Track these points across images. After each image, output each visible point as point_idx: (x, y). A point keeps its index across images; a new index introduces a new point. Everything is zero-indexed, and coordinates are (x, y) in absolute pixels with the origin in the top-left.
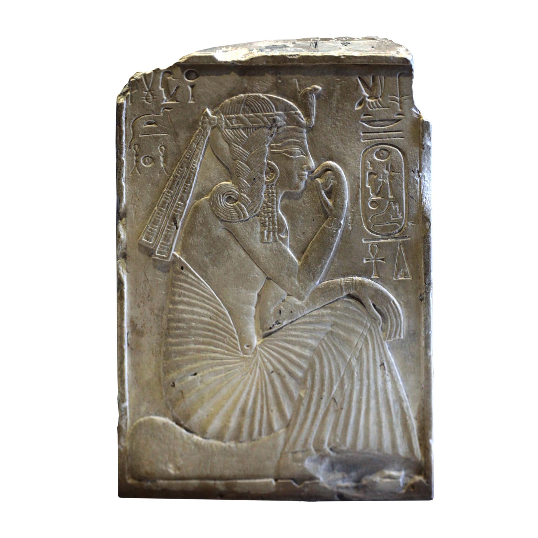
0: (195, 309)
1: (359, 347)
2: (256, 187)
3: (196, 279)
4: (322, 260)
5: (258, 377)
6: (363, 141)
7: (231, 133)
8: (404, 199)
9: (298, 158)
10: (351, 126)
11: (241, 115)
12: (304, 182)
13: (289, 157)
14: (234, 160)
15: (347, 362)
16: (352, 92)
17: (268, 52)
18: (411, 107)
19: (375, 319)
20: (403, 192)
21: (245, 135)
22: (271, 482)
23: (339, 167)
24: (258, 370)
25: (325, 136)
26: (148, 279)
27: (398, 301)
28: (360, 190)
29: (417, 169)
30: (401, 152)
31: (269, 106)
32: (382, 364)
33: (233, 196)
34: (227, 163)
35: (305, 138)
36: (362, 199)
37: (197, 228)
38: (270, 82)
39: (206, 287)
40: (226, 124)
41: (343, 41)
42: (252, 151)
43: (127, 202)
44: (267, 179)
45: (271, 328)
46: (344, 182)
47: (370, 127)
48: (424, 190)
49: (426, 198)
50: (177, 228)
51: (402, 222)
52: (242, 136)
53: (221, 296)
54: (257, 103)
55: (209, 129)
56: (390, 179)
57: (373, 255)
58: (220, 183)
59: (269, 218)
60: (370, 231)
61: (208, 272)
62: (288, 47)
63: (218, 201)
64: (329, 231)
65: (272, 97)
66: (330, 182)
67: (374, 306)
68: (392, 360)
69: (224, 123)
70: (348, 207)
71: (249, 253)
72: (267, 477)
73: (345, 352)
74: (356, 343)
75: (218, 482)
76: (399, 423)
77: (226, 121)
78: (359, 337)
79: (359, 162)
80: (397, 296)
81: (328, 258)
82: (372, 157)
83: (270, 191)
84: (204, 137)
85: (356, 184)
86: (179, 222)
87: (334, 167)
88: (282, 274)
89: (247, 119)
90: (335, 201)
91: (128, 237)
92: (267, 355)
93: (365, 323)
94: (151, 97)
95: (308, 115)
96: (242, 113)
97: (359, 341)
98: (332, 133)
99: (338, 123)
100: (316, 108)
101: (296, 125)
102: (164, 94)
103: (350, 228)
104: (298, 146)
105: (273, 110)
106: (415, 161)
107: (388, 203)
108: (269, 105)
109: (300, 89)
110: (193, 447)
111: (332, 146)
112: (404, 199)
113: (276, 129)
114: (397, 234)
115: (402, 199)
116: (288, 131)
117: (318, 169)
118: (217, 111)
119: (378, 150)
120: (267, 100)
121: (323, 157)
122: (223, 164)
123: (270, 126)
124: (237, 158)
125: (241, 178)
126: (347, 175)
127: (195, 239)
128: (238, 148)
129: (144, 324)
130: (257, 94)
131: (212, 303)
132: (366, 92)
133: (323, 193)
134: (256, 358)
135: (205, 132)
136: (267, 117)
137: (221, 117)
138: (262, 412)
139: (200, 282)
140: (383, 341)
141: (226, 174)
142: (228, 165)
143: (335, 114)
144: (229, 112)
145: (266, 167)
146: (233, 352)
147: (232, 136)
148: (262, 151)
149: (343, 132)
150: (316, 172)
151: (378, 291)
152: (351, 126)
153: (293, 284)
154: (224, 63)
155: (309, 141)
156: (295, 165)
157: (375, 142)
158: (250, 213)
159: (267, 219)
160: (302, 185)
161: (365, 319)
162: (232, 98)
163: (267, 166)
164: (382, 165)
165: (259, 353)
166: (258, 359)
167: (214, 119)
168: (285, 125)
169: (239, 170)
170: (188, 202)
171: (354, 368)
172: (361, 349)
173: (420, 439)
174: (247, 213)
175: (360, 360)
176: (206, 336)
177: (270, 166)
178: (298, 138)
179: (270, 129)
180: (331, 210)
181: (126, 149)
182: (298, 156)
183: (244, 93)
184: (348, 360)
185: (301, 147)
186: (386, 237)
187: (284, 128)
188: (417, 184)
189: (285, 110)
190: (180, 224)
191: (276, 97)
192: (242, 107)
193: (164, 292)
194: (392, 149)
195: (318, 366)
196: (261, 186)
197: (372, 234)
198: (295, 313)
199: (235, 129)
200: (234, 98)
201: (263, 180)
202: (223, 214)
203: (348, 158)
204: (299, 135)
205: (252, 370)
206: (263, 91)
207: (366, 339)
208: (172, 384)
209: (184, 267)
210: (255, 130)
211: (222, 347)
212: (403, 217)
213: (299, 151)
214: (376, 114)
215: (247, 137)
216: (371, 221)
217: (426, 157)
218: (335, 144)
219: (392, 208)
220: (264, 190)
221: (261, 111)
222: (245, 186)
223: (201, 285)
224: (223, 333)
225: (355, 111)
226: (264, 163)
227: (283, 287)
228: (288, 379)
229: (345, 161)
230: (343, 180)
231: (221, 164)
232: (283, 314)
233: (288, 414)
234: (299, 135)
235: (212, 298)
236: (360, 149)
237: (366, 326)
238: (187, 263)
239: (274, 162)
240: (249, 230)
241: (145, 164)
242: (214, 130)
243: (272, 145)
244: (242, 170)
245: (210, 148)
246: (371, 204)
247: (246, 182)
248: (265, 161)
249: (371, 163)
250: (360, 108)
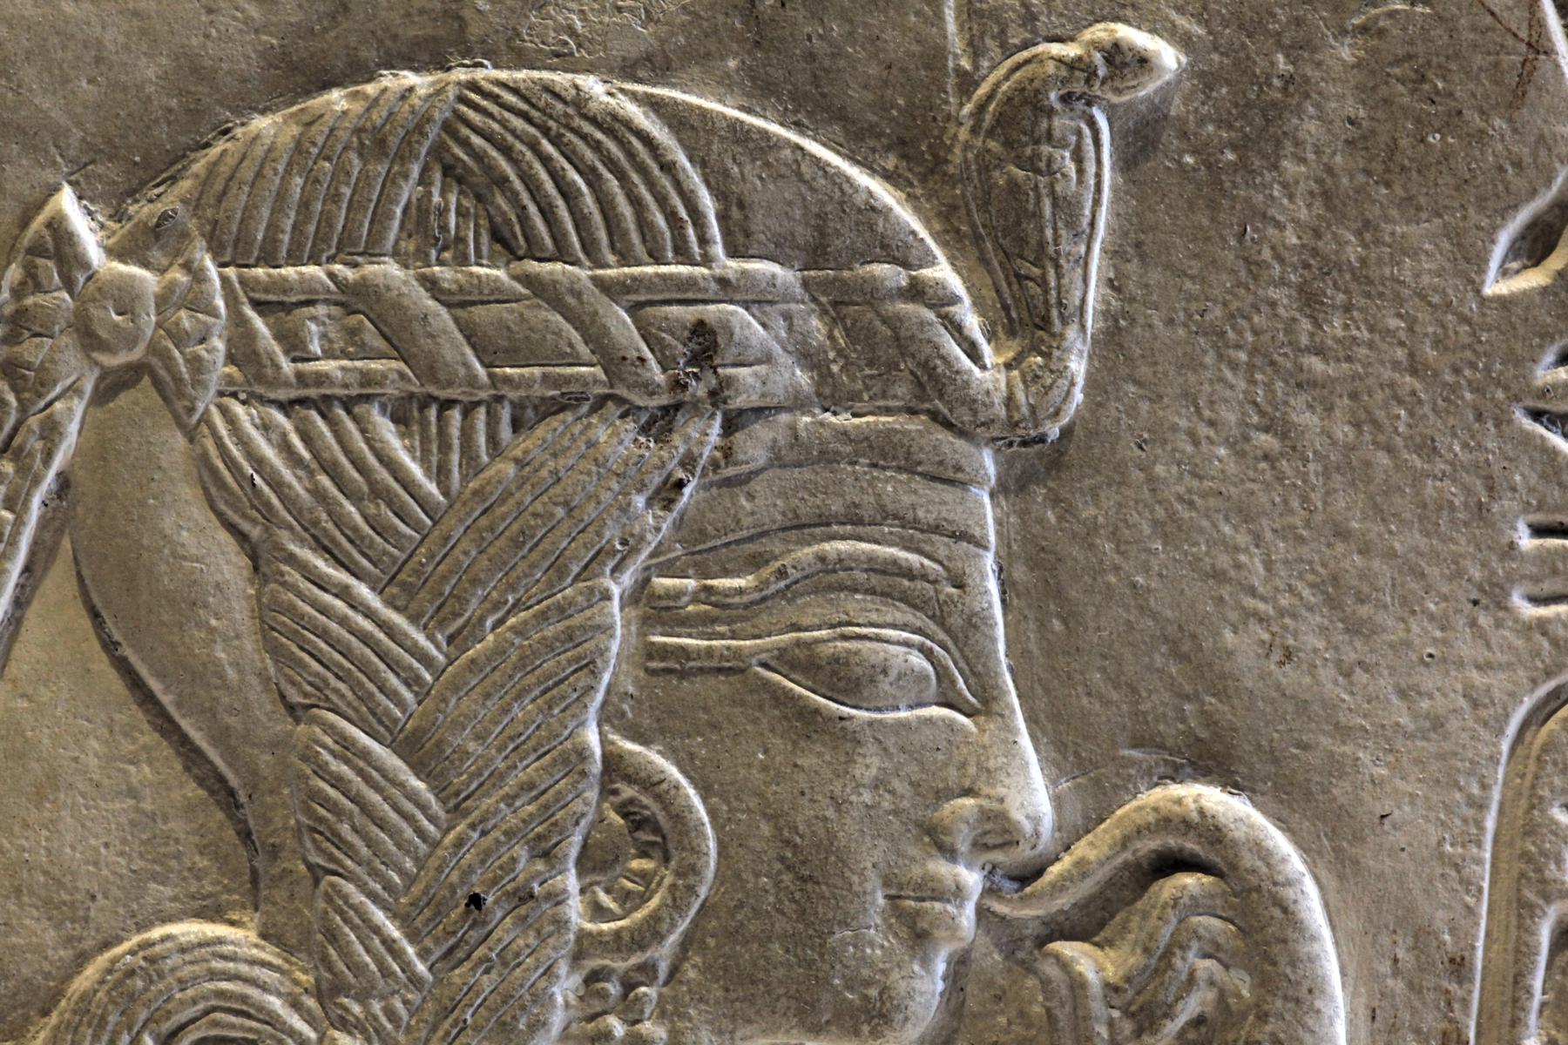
2: (487, 982)
6: (1530, 611)
7: (286, 448)
9: (903, 725)
11: (389, 270)
12: (941, 967)
13: (817, 711)
14: (291, 708)
21: (416, 470)
25: (1171, 529)
31: (662, 201)
34: (221, 736)
35: (986, 548)
40: (243, 352)
42: (473, 630)
44: (598, 912)
46: (1316, 988)
52: (384, 475)
54: (546, 160)
55: (73, 390)
58: (142, 927)
65: (704, 114)
69: (219, 344)
77: (238, 320)
79: (1481, 806)
83: (618, 1028)
84: (22, 470)
87: (1239, 833)
89: (443, 317)
96: (395, 254)
98: (1245, 514)
99: (1306, 419)
100: (1114, 254)
101: (912, 412)
104: (909, 616)
105: (704, 241)
108: (665, 182)
109: (976, 51)
113: (716, 429)
116: (827, 457)
117: (1081, 849)
118: (164, 217)
121: (1137, 744)
122: (183, 743)
123: (664, 400)
124: (320, 686)
125: (350, 888)
126: (1353, 923)
128: (344, 593)
135: (34, 422)
136: (634, 309)
137: (198, 276)
141: (202, 850)
142: (231, 755)
144: (274, 228)
145: (592, 795)
147: (287, 474)
148: (569, 636)
149: (1346, 505)
150: (1059, 887)
152: (1428, 448)
155: (1020, 573)
156: (867, 797)
162: (317, 102)
163: (607, 792)
167: (125, 298)
168: (798, 403)
169: (326, 802)
177: (628, 792)
178: (915, 531)
179: (660, 424)
182: (903, 714)
183: (430, 56)
185: (941, 621)
187: (793, 428)
189: (815, 254)
192: (408, 191)
196: (527, 974)
199: (323, 406)
200: (337, 99)
201: (561, 924)
204: (930, 502)
206: (622, 48)
210: (517, 425)
213: (918, 661)
215: (432, 488)
218: (1262, 619)
220: (557, 1020)
221: (589, 247)
222: (386, 972)
225: (1483, 301)
226: (582, 754)
229: (1341, 791)
230: (1312, 959)
231: (166, 750)
234: (930, 502)
236: (1498, 683)
239: (672, 753)
242: (124, 399)
243: (663, 583)
245: (71, 587)
248: (592, 737)
250: (1533, 279)
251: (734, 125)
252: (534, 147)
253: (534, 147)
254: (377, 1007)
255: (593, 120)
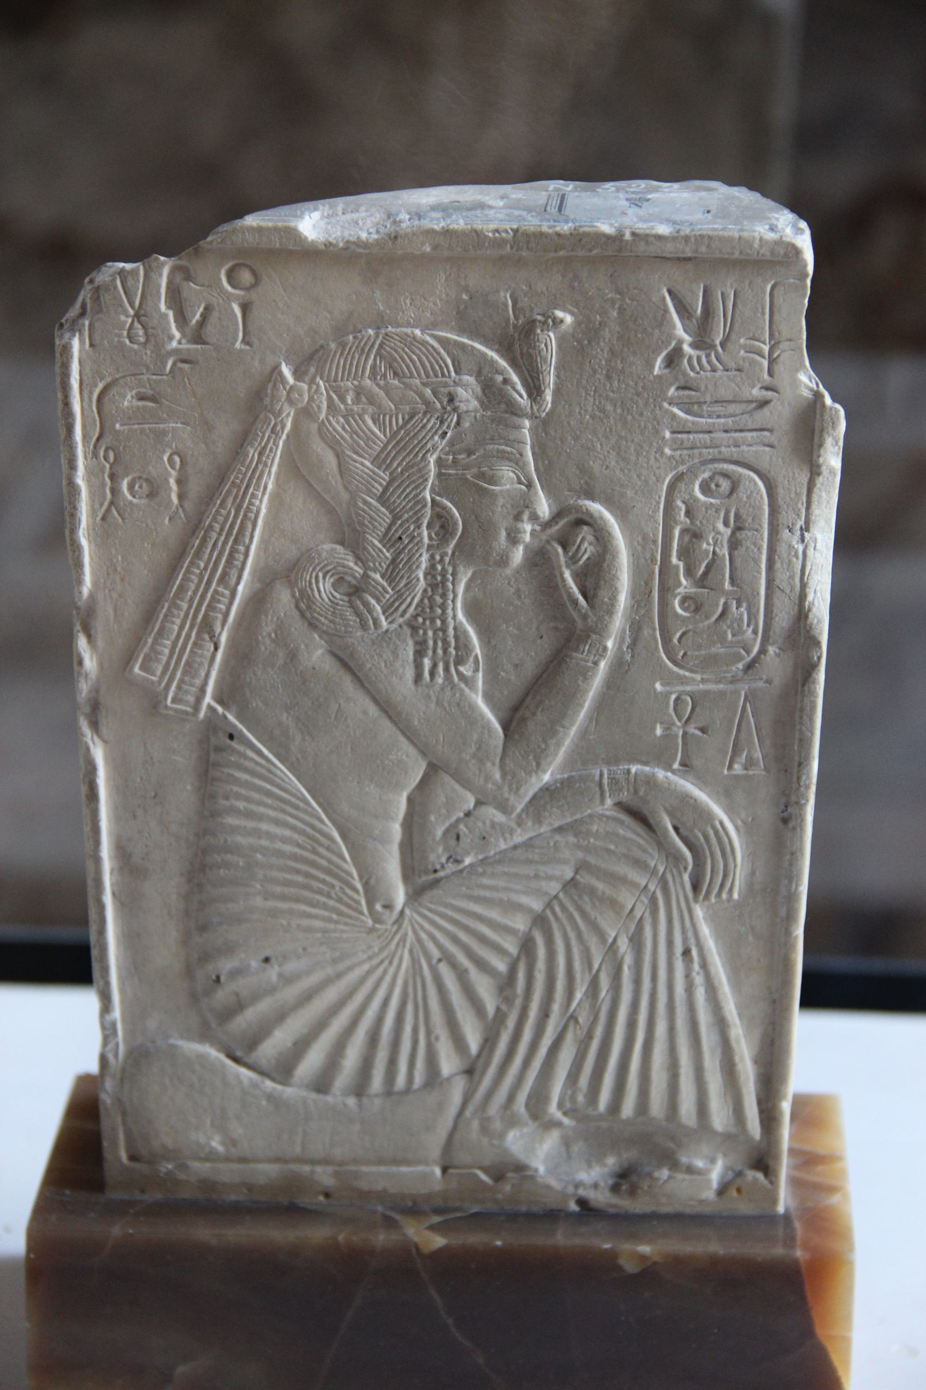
0: (264, 826)
1: (638, 914)
3: (263, 762)
4: (557, 727)
5: (407, 971)
10: (641, 414)
13: (486, 489)
15: (608, 944)
16: (649, 329)
17: (438, 219)
18: (797, 371)
19: (675, 858)
20: (760, 578)
21: (377, 431)
22: (433, 1173)
23: (607, 515)
24: (406, 956)
26: (152, 758)
27: (732, 821)
29: (801, 523)
31: (437, 363)
32: (686, 953)
33: (348, 578)
37: (263, 649)
38: (441, 300)
39: (287, 779)
41: (633, 193)
43: (95, 583)
45: (435, 871)
47: (690, 418)
48: (813, 572)
50: (216, 648)
51: (753, 646)
53: (321, 800)
54: (406, 353)
59: (435, 633)
60: (675, 663)
61: (292, 747)
62: (491, 207)
63: (312, 590)
64: (577, 664)
65: (447, 338)
67: (676, 829)
68: (710, 944)
71: (387, 708)
72: (426, 1162)
73: (603, 924)
74: (630, 907)
75: (319, 1169)
76: (718, 1068)
78: (637, 894)
80: (730, 810)
81: (572, 725)
86: (220, 634)
87: (596, 515)
88: (464, 755)
91: (101, 665)
92: (427, 926)
93: (653, 864)
94: (141, 332)
95: (535, 390)
97: (638, 903)
102: (173, 325)
103: (628, 657)
105: (449, 372)
106: (796, 504)
107: (722, 601)
110: (264, 1103)
115: (758, 594)
119: (706, 475)
120: (433, 347)
124: (357, 486)
127: (259, 673)
128: (362, 464)
129: (147, 854)
130: (409, 330)
131: (302, 815)
132: (685, 331)
134: (402, 932)
138: (415, 1042)
139: (272, 768)
140: (693, 905)
143: (604, 385)
146: (350, 917)
151: (686, 800)
153: (488, 778)
154: (323, 247)
158: (390, 619)
159: (430, 633)
160: (518, 555)
161: (652, 856)
165: (410, 920)
166: (406, 934)
169: (360, 516)
170: (240, 588)
171: (622, 958)
172: (641, 918)
173: (759, 1103)
174: (383, 618)
175: (636, 941)
176: (288, 883)
177: (438, 509)
180: (585, 617)
181: (86, 458)
184: (610, 940)
185: (517, 464)
188: (797, 558)
190: (224, 639)
191: (456, 337)
193: (189, 787)
195: (541, 952)
198: (492, 840)
202: (326, 618)
203: (629, 493)
205: (393, 957)
207: (653, 900)
208: (214, 977)
209: (235, 734)
211: (325, 907)
213: (512, 475)
214: (706, 386)
215: (382, 436)
217: (824, 494)
223: (275, 775)
224: (328, 879)
227: (466, 784)
228: (474, 974)
232: (465, 841)
233: (474, 1042)
235: (301, 805)
237: (654, 872)
238: (240, 726)
240: (387, 655)
241: (134, 497)
244: (372, 518)
246: (682, 603)
247: (380, 546)
251: (456, 342)
252: (403, 350)
253: (403, 350)
254: (377, 564)
255: (418, 342)
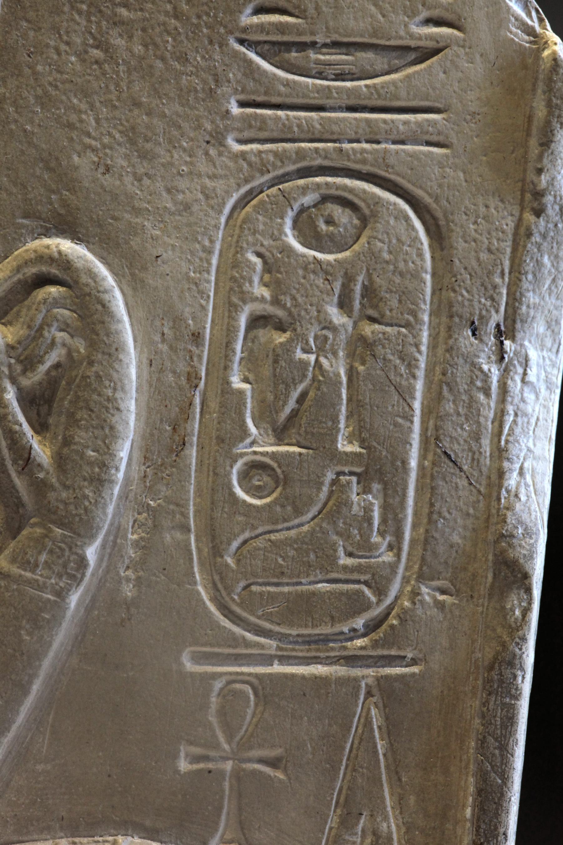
6: (237, 147)
8: (413, 463)
10: (183, 59)
20: (410, 430)
28: (197, 400)
29: (496, 318)
30: (424, 223)
36: (201, 447)
46: (120, 348)
48: (518, 430)
49: (521, 473)
51: (389, 581)
56: (351, 355)
57: (230, 738)
66: (53, 343)
70: (127, 480)
79: (210, 252)
82: (277, 236)
85: (182, 367)
87: (79, 264)
90: (67, 442)
98: (85, 93)
106: (490, 274)
107: (330, 476)
111: (76, 158)
112: (413, 463)
114: (359, 642)
115: (405, 463)
119: (308, 199)
133: (10, 395)
157: (301, 155)
164: (320, 282)
186: (301, 651)
188: (488, 394)
194: (378, 201)
197: (237, 630)
212: (398, 556)
216: (238, 561)
217: (546, 260)
218: (94, 150)
219: (348, 504)
230: (118, 332)
236: (219, 185)
246: (245, 477)
249: (268, 268)
